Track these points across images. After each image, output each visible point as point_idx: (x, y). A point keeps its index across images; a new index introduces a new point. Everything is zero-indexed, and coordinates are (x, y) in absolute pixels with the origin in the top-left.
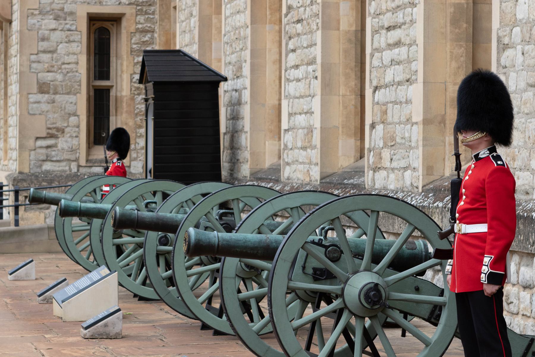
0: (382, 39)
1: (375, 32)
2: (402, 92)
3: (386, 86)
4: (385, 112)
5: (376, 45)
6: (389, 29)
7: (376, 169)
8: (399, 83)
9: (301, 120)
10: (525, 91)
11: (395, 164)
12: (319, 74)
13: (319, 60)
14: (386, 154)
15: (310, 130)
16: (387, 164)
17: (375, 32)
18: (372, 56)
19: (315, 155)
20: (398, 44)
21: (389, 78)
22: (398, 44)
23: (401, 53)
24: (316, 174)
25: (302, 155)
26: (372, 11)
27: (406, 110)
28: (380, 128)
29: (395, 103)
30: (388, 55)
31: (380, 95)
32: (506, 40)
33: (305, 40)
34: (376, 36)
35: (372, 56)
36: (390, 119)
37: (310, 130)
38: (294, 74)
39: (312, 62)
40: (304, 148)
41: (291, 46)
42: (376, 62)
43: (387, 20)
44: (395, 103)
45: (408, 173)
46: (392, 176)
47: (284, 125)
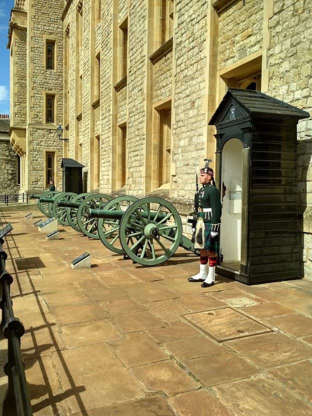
0: (132, 155)
1: (129, 152)
2: (138, 169)
3: (133, 167)
4: (133, 174)
5: (130, 156)
6: (134, 151)
7: (130, 190)
8: (137, 166)
9: (105, 177)
10: (183, 167)
11: (136, 188)
12: (111, 165)
13: (111, 161)
14: (133, 186)
15: (108, 180)
16: (133, 189)
17: (129, 152)
18: (128, 159)
19: (110, 186)
20: (137, 155)
21: (134, 164)
22: (137, 155)
23: (139, 158)
24: (110, 191)
25: (106, 186)
26: (128, 147)
27: (139, 174)
28: (131, 179)
29: (136, 172)
30: (133, 159)
31: (131, 170)
32: (176, 152)
33: (107, 156)
34: (130, 154)
35: (128, 159)
36: (134, 176)
37: (108, 180)
38: (103, 165)
39: (109, 162)
40: (106, 184)
41: (102, 157)
42: (129, 161)
43: (133, 149)
44: (136, 172)
45: (140, 192)
46: (135, 192)
47: (100, 179)
